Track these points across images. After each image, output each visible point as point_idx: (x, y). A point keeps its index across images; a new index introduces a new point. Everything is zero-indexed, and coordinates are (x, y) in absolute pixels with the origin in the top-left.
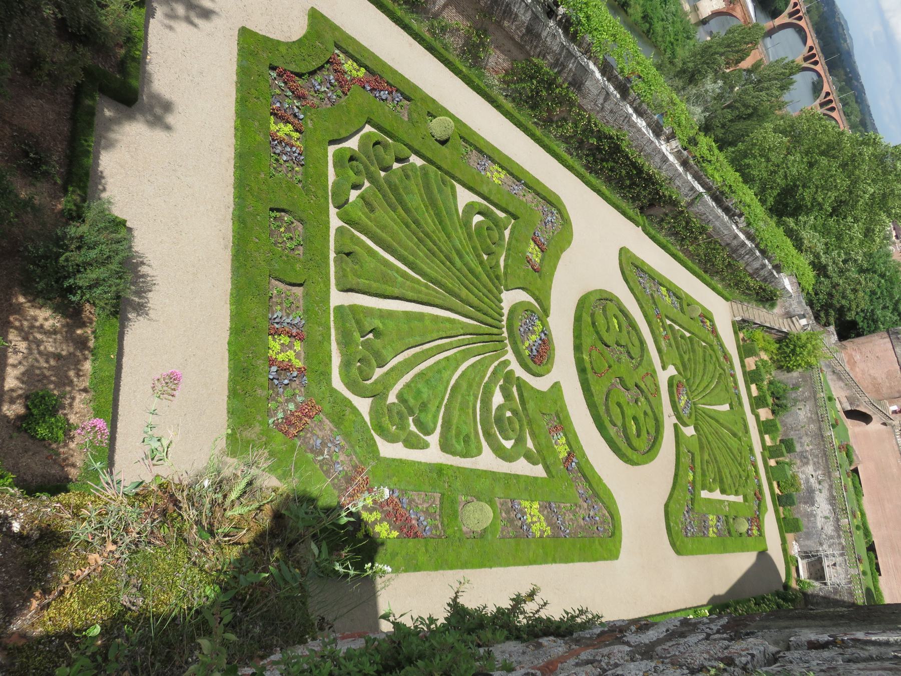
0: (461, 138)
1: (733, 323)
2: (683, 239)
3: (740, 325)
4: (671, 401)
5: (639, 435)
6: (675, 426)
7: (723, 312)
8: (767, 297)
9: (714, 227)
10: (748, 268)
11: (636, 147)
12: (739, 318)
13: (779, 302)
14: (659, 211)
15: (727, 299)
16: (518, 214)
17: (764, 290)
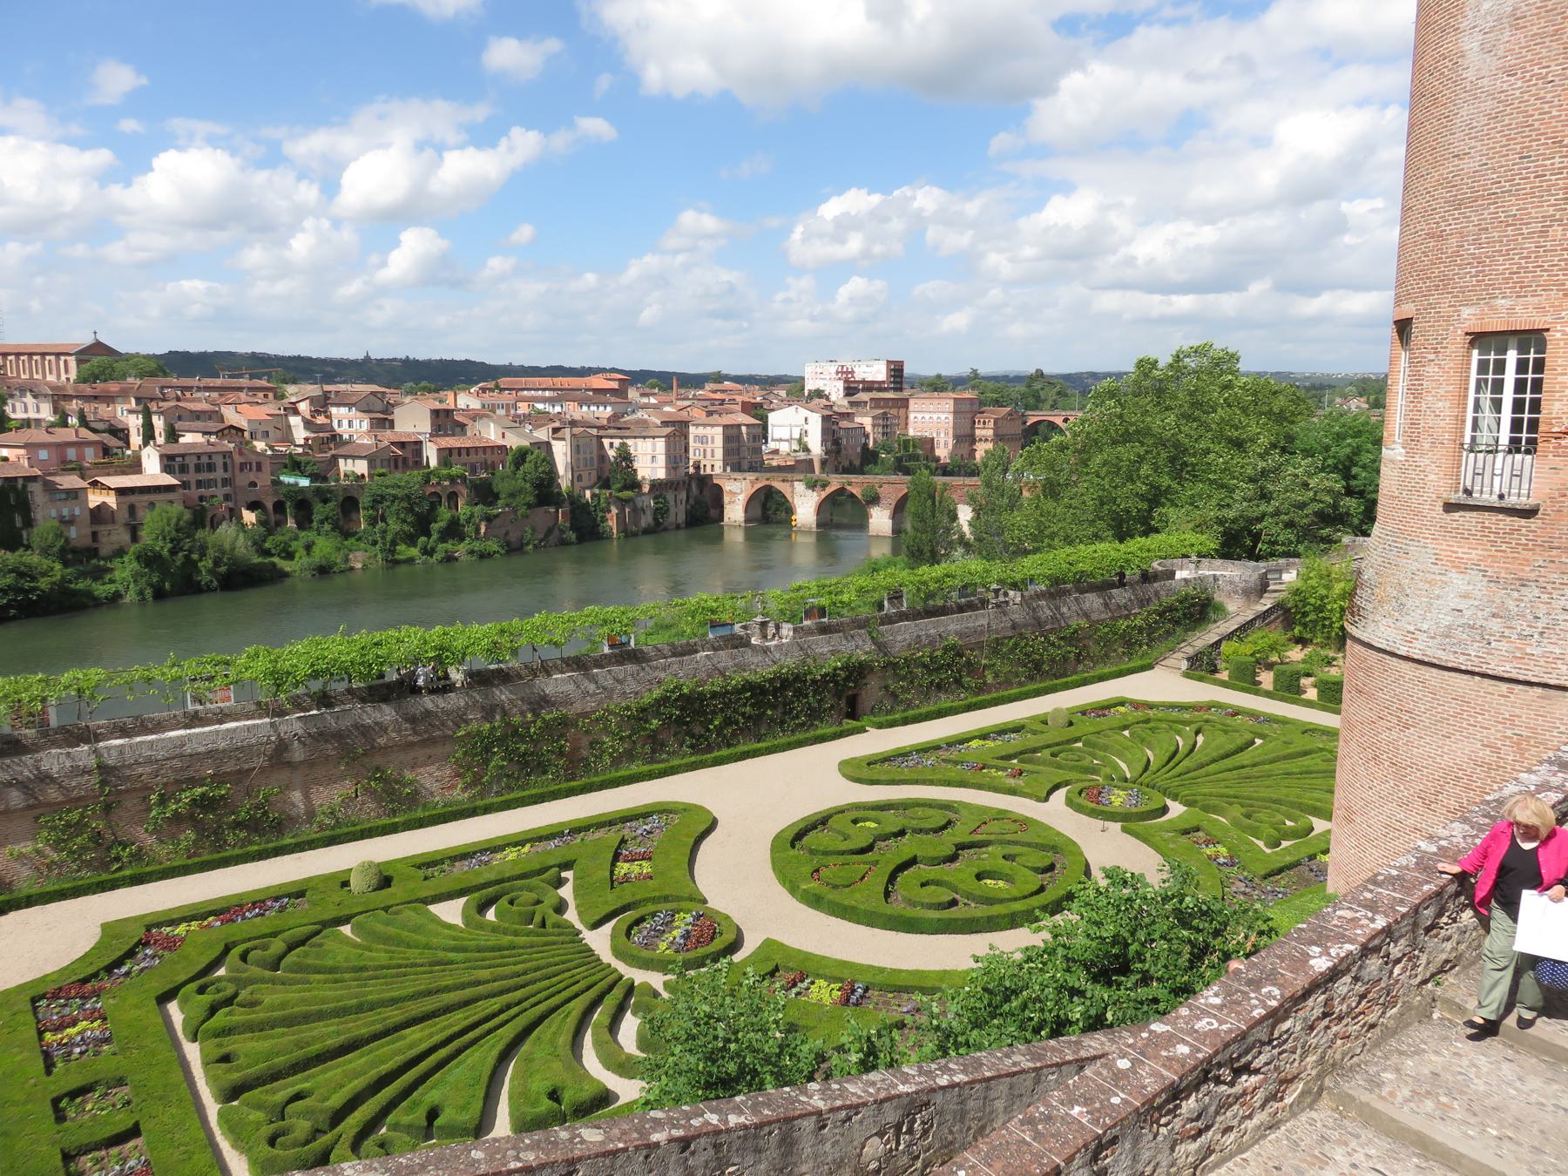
0: (419, 868)
1: (1186, 675)
2: (958, 682)
3: (1203, 666)
4: (1089, 815)
5: (1009, 879)
6: (1124, 830)
7: (1163, 683)
8: (1199, 609)
9: (956, 633)
10: (1094, 617)
11: (709, 676)
12: (1184, 665)
13: (1218, 597)
14: (872, 690)
15: (1150, 667)
16: (569, 857)
17: (1171, 609)
